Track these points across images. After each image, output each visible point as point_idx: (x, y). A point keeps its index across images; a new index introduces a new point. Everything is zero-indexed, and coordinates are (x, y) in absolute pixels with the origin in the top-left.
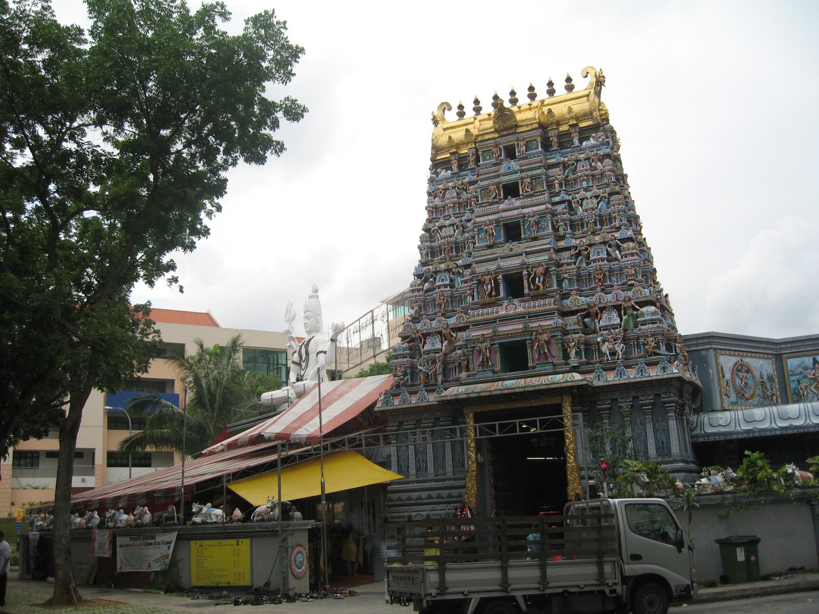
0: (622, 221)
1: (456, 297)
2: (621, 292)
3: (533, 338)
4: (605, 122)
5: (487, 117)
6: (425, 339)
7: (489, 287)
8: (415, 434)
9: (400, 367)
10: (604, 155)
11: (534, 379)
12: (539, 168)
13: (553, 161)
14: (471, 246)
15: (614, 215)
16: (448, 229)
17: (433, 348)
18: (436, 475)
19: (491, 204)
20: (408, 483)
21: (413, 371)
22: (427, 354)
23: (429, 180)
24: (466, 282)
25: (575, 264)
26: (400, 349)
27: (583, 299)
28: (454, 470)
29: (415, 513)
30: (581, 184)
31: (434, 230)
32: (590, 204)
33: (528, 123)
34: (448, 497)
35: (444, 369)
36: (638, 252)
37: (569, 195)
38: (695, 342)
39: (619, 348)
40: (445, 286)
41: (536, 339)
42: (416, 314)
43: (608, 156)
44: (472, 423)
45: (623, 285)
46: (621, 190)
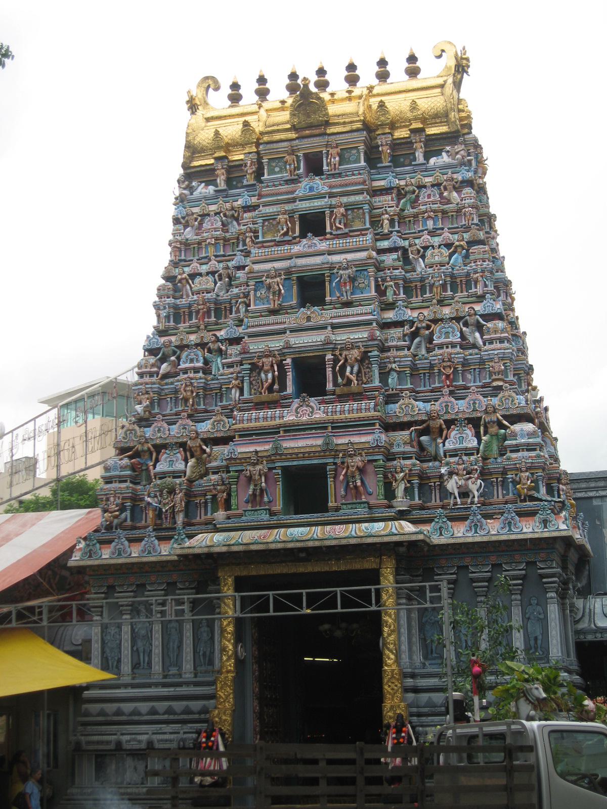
0: (486, 286)
1: (211, 389)
2: (481, 397)
3: (338, 461)
4: (466, 131)
5: (280, 105)
6: (158, 453)
7: (270, 375)
8: (163, 604)
9: (115, 497)
10: (462, 182)
11: (337, 527)
12: (360, 192)
13: (382, 183)
14: (242, 309)
15: (475, 276)
16: (204, 278)
17: (171, 469)
18: (165, 677)
19: (278, 244)
20: (117, 687)
21: (135, 504)
22: (160, 478)
23: (176, 198)
24: (230, 366)
25: (409, 349)
26: (115, 468)
27: (421, 404)
28: (195, 668)
29: (128, 737)
30: (425, 224)
31: (182, 279)
32: (437, 256)
33: (347, 120)
34: (183, 713)
35: (188, 504)
36: (510, 337)
37: (405, 239)
38: (584, 485)
39: (475, 486)
40: (196, 370)
41: (343, 463)
42: (145, 412)
43: (470, 183)
44: (231, 592)
45: (482, 387)
46: (487, 238)
